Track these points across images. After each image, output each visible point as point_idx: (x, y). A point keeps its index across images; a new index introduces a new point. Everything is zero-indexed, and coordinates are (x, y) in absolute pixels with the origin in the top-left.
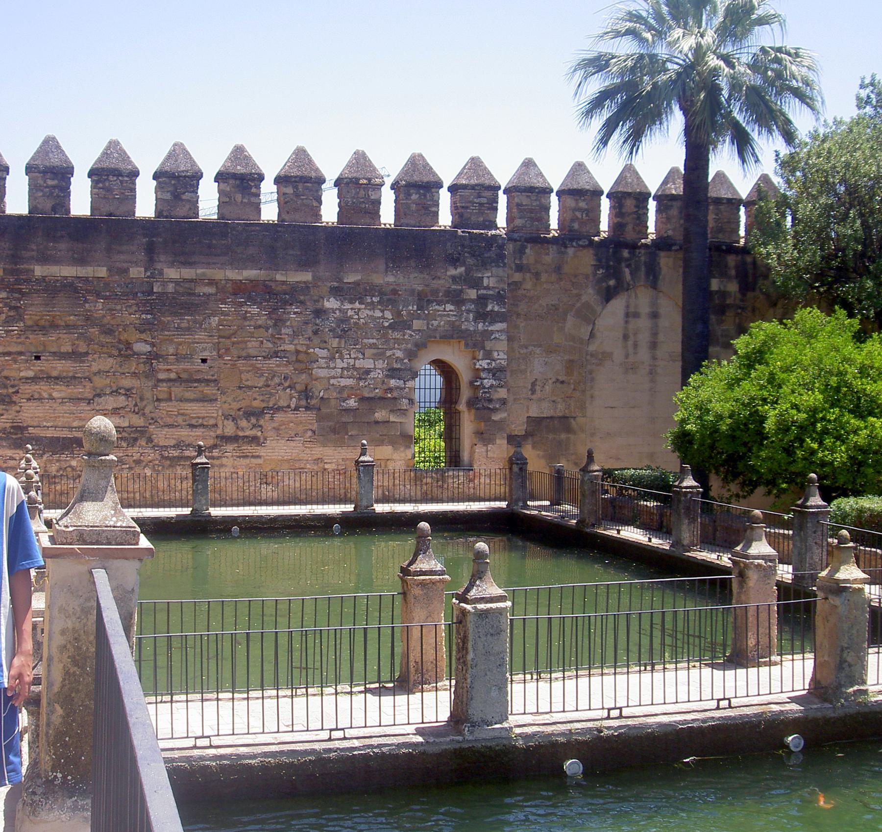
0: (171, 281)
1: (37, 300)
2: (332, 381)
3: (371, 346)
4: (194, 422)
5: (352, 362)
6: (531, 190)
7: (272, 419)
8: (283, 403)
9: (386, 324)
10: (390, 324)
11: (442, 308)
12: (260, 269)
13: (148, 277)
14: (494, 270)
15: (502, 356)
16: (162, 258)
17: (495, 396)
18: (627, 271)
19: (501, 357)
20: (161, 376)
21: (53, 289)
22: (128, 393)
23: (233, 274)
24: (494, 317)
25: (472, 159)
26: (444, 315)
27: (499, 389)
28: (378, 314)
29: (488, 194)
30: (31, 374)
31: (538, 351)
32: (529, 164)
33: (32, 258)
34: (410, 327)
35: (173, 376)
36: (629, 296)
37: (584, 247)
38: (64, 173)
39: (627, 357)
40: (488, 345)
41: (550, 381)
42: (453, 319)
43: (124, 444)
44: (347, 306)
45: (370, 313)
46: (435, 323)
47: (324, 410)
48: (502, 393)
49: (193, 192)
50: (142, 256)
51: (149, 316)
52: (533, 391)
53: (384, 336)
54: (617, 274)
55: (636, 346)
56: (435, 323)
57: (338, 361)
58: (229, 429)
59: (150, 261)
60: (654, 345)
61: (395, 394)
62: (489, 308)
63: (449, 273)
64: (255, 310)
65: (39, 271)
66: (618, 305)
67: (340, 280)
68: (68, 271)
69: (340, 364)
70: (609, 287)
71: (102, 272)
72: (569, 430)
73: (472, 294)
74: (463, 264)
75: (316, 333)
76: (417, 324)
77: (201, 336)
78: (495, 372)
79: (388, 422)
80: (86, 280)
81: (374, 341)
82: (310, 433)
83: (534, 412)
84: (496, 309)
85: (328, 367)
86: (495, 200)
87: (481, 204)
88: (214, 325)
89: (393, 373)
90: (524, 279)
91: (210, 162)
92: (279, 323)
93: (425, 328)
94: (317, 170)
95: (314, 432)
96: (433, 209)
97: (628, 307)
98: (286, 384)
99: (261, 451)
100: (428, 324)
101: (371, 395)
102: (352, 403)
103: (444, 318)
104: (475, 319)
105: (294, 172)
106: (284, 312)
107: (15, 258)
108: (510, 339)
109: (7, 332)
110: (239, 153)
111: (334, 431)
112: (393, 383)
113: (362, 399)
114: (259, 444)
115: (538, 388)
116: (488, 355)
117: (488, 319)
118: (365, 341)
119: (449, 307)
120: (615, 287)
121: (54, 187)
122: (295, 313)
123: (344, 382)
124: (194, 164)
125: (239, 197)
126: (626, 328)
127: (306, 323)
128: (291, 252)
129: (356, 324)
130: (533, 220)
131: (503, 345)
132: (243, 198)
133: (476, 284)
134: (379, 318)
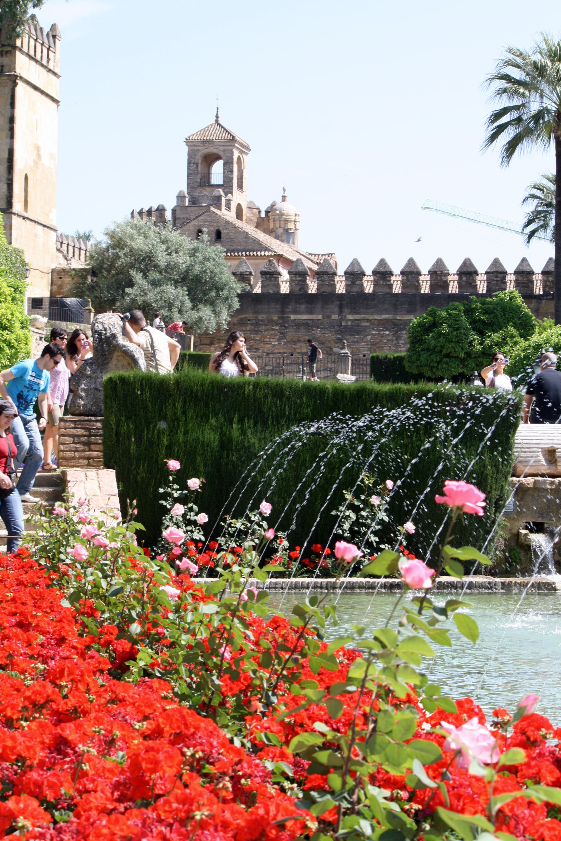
1: (292, 330)
21: (298, 325)
23: (377, 317)
29: (501, 276)
32: (524, 260)
50: (337, 310)
59: (340, 312)
64: (387, 333)
65: (293, 317)
68: (305, 317)
71: (320, 317)
77: (363, 344)
80: (313, 320)
91: (368, 268)
92: (398, 338)
94: (417, 268)
105: (407, 270)
107: (283, 312)
110: (382, 262)
124: (361, 268)
125: (381, 282)
130: (524, 287)
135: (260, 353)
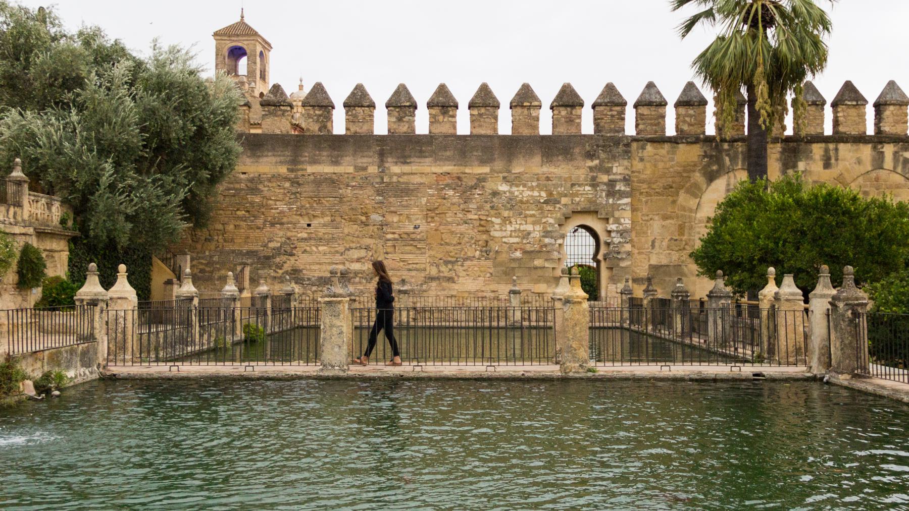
0: (396, 174)
2: (504, 240)
4: (410, 267)
5: (518, 226)
6: (649, 104)
7: (462, 266)
8: (470, 254)
9: (542, 201)
11: (582, 189)
14: (621, 161)
15: (627, 221)
16: (390, 160)
17: (623, 250)
18: (727, 159)
19: (627, 222)
20: (390, 236)
21: (320, 181)
22: (367, 248)
24: (622, 194)
25: (607, 85)
28: (536, 194)
29: (618, 108)
30: (305, 235)
31: (656, 218)
32: (650, 86)
33: (306, 161)
34: (559, 202)
35: (396, 236)
36: (729, 178)
37: (692, 143)
38: (327, 107)
40: (617, 214)
42: (590, 196)
43: (364, 281)
44: (514, 189)
45: (530, 193)
46: (577, 199)
47: (499, 259)
48: (628, 247)
50: (376, 159)
52: (653, 246)
53: (541, 209)
54: (719, 161)
56: (577, 199)
57: (508, 226)
58: (434, 271)
59: (382, 162)
61: (549, 248)
62: (617, 188)
64: (451, 193)
67: (509, 172)
68: (327, 169)
69: (509, 228)
70: (713, 171)
71: (351, 169)
73: (605, 178)
74: (598, 158)
75: (492, 208)
76: (564, 200)
77: (415, 210)
78: (621, 233)
82: (488, 275)
83: (654, 261)
84: (623, 188)
85: (501, 230)
86: (623, 112)
87: (612, 116)
88: (424, 203)
89: (547, 234)
90: (645, 167)
96: (577, 121)
97: (728, 185)
99: (456, 287)
101: (532, 249)
102: (518, 254)
104: (608, 196)
108: (634, 210)
109: (289, 209)
111: (506, 273)
112: (547, 240)
113: (525, 252)
115: (657, 244)
116: (617, 221)
117: (617, 196)
119: (588, 188)
120: (718, 171)
121: (320, 116)
123: (512, 240)
127: (486, 202)
128: (475, 153)
131: (628, 214)
133: (608, 171)
135: (260, 222)
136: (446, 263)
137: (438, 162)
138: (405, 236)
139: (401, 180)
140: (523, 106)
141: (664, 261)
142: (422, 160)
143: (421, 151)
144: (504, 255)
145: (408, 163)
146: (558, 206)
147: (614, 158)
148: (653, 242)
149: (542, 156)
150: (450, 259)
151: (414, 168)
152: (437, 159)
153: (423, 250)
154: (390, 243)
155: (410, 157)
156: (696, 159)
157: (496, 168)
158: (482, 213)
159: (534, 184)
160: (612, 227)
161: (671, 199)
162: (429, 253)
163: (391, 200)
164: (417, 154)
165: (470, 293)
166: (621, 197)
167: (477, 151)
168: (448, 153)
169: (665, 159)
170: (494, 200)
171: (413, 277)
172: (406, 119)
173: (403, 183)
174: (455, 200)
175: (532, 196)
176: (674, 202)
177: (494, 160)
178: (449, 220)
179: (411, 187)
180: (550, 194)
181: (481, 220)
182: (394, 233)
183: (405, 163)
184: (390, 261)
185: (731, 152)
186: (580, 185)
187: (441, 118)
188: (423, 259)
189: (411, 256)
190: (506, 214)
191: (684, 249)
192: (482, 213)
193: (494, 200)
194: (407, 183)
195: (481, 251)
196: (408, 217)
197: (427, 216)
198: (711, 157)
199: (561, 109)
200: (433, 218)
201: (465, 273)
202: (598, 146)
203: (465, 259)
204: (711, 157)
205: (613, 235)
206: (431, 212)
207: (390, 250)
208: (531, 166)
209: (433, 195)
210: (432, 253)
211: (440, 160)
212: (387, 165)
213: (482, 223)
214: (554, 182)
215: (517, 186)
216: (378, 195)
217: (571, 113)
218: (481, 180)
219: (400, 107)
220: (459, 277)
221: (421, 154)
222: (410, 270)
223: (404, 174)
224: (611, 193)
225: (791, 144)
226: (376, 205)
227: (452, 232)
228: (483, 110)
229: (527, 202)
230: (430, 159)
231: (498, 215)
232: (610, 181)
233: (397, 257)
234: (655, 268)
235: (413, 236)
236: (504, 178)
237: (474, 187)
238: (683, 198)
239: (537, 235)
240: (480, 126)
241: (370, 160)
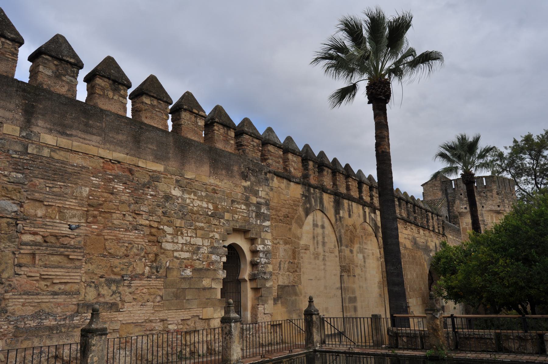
0: (47, 146)
2: (176, 254)
3: (202, 228)
4: (56, 288)
8: (139, 271)
9: (210, 213)
10: (212, 213)
11: (239, 207)
12: (127, 154)
13: (23, 137)
15: (269, 243)
16: (40, 123)
20: (27, 238)
24: (265, 218)
26: (241, 212)
27: (269, 265)
28: (205, 205)
34: (223, 218)
35: (39, 239)
39: (315, 249)
40: (263, 235)
41: (287, 263)
42: (245, 215)
44: (186, 196)
47: (170, 278)
48: (270, 268)
49: (73, 77)
50: (19, 116)
51: (20, 176)
52: (280, 267)
55: (317, 243)
56: (236, 216)
57: (180, 237)
58: (91, 295)
59: (27, 124)
60: (324, 244)
62: (262, 211)
63: (243, 184)
64: (120, 187)
66: (310, 218)
67: (182, 176)
69: (181, 240)
72: (296, 294)
73: (254, 200)
74: (249, 180)
75: (164, 213)
76: (227, 216)
77: (71, 203)
78: (267, 253)
79: (211, 288)
81: (202, 225)
82: (158, 299)
84: (265, 212)
85: (173, 242)
87: (254, 146)
88: (85, 194)
93: (231, 219)
95: (162, 297)
97: (314, 220)
98: (142, 255)
99: (120, 317)
100: (233, 216)
101: (201, 267)
102: (188, 272)
103: (241, 214)
106: (143, 193)
114: (118, 311)
115: (282, 266)
116: (263, 243)
118: (197, 224)
119: (243, 207)
122: (151, 195)
126: (314, 233)
127: (159, 206)
129: (192, 210)
131: (269, 236)
132: (114, 95)
133: (256, 194)
134: (205, 208)
136: (109, 282)
137: (108, 146)
138: (53, 240)
139: (56, 156)
140: (191, 112)
141: (286, 283)
142: (88, 137)
143: (86, 125)
144: (175, 273)
145: (68, 135)
146: (222, 220)
147: (259, 183)
148: (280, 264)
149: (210, 166)
150: (113, 277)
151: (76, 144)
152: (106, 141)
153: (77, 263)
154: (26, 250)
155: (71, 127)
156: (299, 196)
157: (170, 168)
158: (154, 218)
159: (204, 194)
160: (260, 247)
161: (288, 226)
162: (86, 267)
163: (37, 181)
164: (81, 126)
165: (136, 324)
166: (265, 220)
167: (152, 143)
168: (120, 137)
169: (284, 192)
170: (167, 204)
171: (59, 305)
172: (67, 78)
173: (58, 161)
174: (125, 198)
175: (201, 207)
176: (290, 229)
177: (169, 158)
178: (115, 222)
179: (70, 169)
180: (216, 208)
181: (151, 227)
182: (35, 234)
183: (63, 134)
184: (23, 280)
185: (314, 196)
186: (238, 203)
187: (111, 94)
188: (77, 276)
189: (59, 272)
190: (178, 223)
191: (296, 271)
192: (154, 218)
193: (167, 204)
194: (63, 162)
195: (151, 267)
196: (61, 211)
197: (86, 214)
198: (306, 197)
199: (221, 127)
200: (95, 217)
201: (131, 297)
202: (249, 169)
203: (134, 277)
204: (306, 197)
205: (261, 255)
206: (94, 209)
207: (25, 260)
208: (199, 173)
209: (98, 187)
210: (91, 267)
211: (111, 142)
212: (36, 129)
213: (153, 230)
214: (219, 195)
215: (189, 193)
216: (17, 170)
217: (227, 134)
218: (155, 178)
219: (61, 60)
220: (123, 301)
221: (87, 129)
222: (55, 294)
223: (61, 149)
224: (259, 215)
225: (337, 198)
226: (10, 187)
227: (118, 240)
228: (155, 102)
229: (197, 212)
230: (98, 138)
231: (170, 224)
232: (258, 203)
233: (35, 272)
234: (282, 288)
235: (66, 241)
236: (177, 181)
237: (147, 186)
238: (294, 226)
239: (205, 250)
240: (152, 118)
241: (8, 114)
